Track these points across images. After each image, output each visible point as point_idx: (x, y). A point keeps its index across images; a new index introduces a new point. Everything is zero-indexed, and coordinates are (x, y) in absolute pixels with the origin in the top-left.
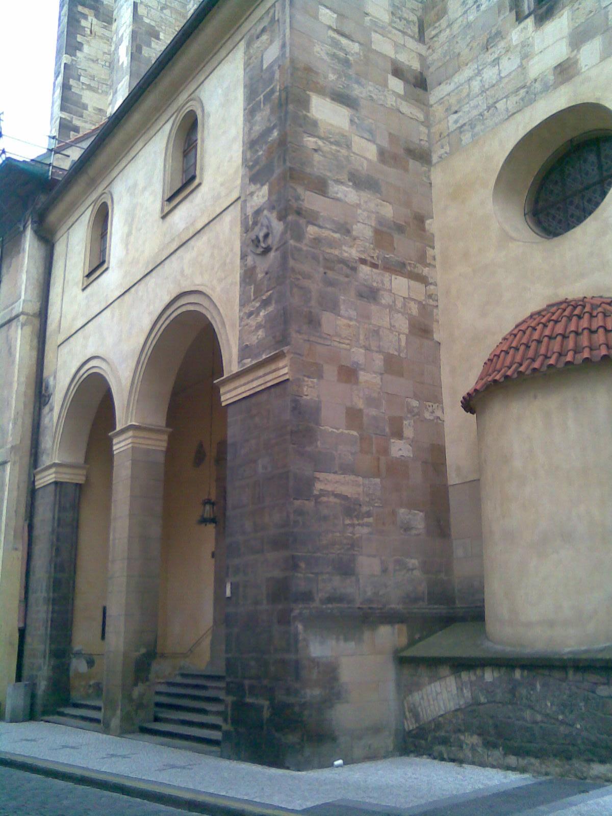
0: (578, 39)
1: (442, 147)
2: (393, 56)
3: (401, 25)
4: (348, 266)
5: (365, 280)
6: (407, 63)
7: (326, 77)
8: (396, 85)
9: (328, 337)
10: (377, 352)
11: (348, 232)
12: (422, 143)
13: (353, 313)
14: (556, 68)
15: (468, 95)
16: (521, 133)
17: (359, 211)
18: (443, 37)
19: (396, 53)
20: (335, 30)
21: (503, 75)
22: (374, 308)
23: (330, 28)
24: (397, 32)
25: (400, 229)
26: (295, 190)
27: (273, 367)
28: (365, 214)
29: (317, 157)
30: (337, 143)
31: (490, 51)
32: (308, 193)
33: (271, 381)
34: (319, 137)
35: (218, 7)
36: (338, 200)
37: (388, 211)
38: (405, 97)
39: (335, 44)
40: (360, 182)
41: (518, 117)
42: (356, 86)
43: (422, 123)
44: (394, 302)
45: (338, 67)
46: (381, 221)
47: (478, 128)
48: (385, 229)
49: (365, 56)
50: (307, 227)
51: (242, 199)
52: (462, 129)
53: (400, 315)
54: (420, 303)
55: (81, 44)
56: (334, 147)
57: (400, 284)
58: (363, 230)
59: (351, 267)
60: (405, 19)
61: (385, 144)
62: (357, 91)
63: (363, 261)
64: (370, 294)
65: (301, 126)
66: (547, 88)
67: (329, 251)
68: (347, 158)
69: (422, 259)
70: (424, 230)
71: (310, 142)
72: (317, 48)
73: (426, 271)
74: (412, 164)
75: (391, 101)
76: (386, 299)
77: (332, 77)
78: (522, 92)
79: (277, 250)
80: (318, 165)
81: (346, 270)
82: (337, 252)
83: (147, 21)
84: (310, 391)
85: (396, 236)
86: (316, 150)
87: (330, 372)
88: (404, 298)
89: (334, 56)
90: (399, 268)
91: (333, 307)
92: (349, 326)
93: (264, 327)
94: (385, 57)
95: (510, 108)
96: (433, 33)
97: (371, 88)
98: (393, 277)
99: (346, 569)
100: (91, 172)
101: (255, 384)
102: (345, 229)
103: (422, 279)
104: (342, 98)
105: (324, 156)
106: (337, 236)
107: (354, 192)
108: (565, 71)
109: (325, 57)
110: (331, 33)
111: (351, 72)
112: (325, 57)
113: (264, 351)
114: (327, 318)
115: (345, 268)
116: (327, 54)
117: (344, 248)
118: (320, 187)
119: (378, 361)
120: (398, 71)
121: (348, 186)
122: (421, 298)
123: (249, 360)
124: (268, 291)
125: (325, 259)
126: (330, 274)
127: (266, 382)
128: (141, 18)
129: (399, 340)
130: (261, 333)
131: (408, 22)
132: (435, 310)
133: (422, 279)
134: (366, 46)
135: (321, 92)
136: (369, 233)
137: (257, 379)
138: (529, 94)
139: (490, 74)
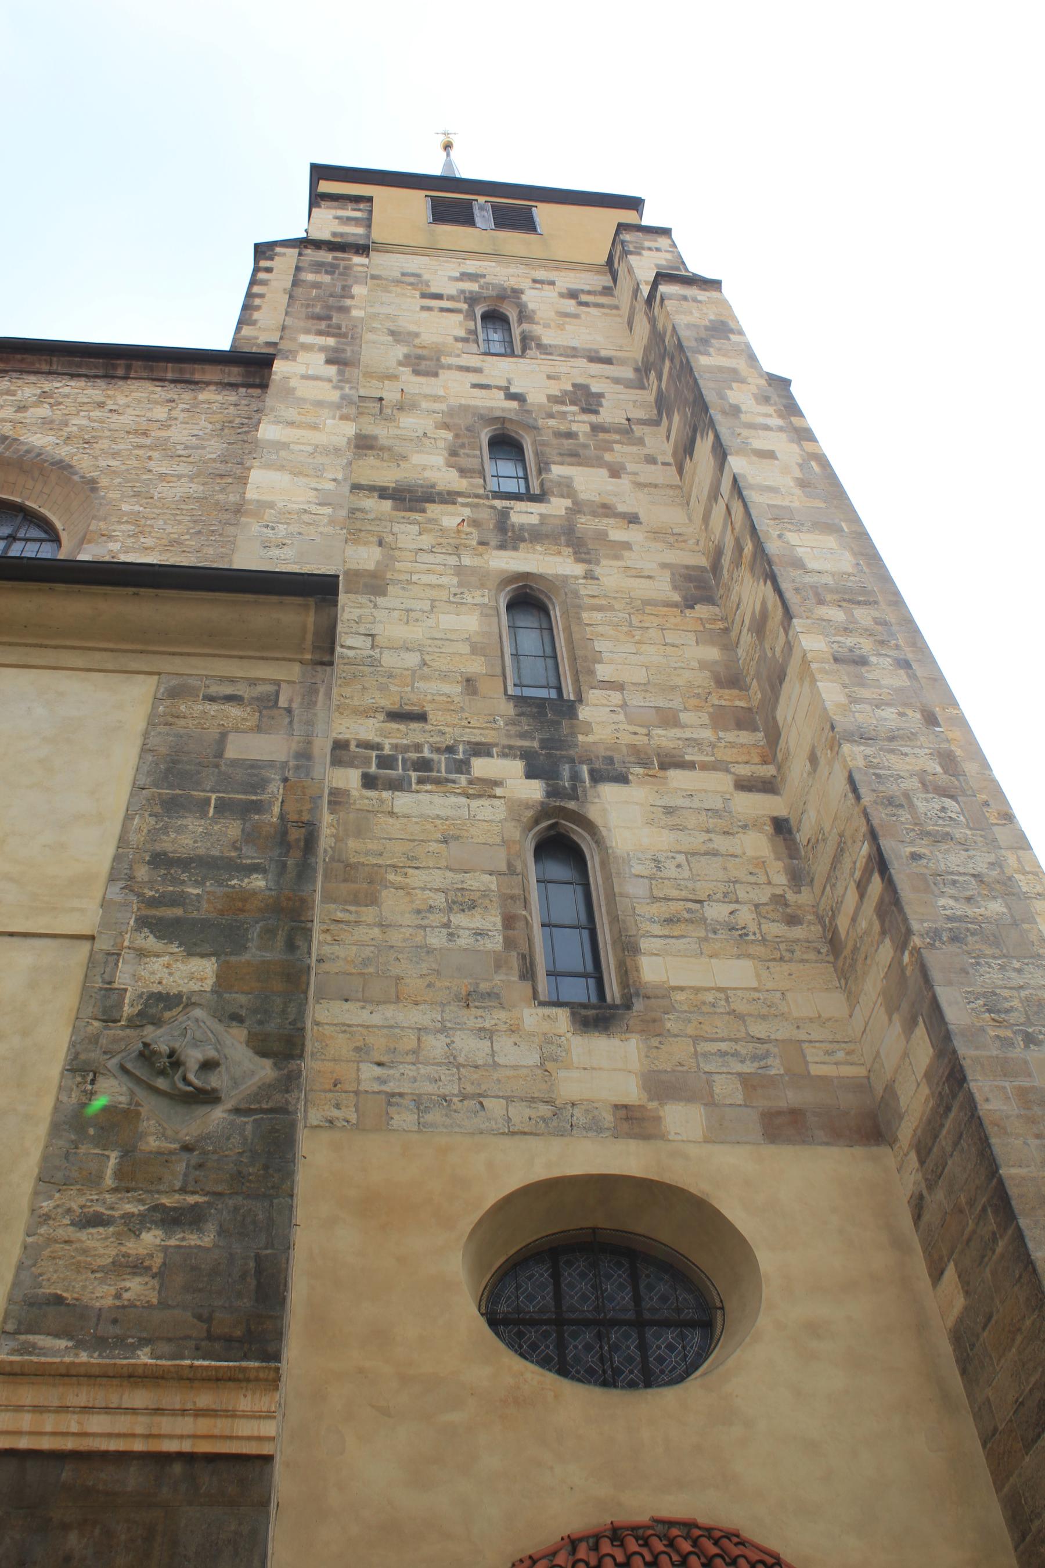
0: (664, 1087)
1: (338, 1106)
14: (616, 1107)
15: (415, 1052)
16: (540, 1173)
18: (363, 933)
21: (500, 1060)
27: (205, 1399)
31: (473, 1011)
33: (171, 1437)
35: (136, 594)
41: (534, 1144)
47: (434, 1116)
51: (103, 944)
52: (394, 1100)
66: (595, 1127)
78: (544, 1110)
79: (237, 1111)
93: (159, 1275)
95: (515, 1120)
96: (340, 915)
101: (97, 1423)
108: (633, 1122)
113: (144, 1342)
123: (62, 1343)
124: (183, 1190)
127: (230, 1438)
130: (136, 1288)
137: (107, 1410)
138: (560, 1120)
139: (469, 1046)
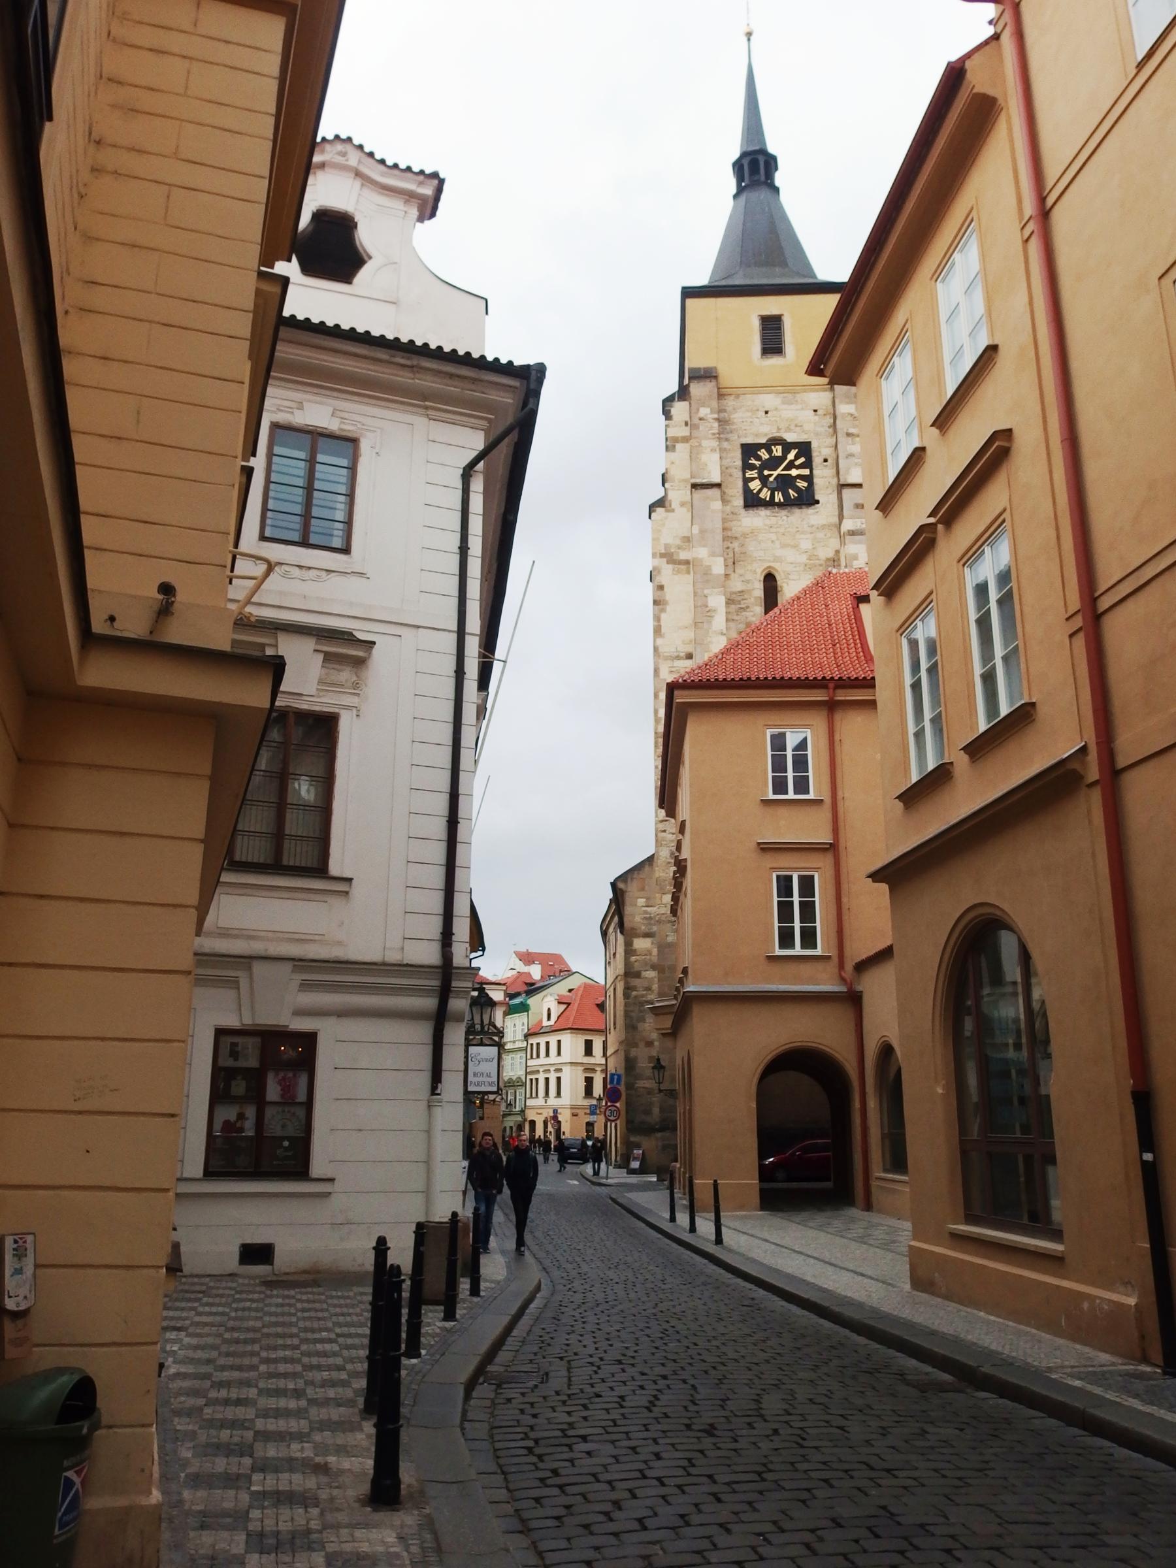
39: (646, 912)
80: (637, 967)
84: (634, 1052)
87: (641, 1045)
89: (646, 918)
91: (644, 1021)
99: (648, 1112)
102: (649, 989)
104: (647, 935)
114: (640, 1026)
118: (638, 975)
135: (638, 936)
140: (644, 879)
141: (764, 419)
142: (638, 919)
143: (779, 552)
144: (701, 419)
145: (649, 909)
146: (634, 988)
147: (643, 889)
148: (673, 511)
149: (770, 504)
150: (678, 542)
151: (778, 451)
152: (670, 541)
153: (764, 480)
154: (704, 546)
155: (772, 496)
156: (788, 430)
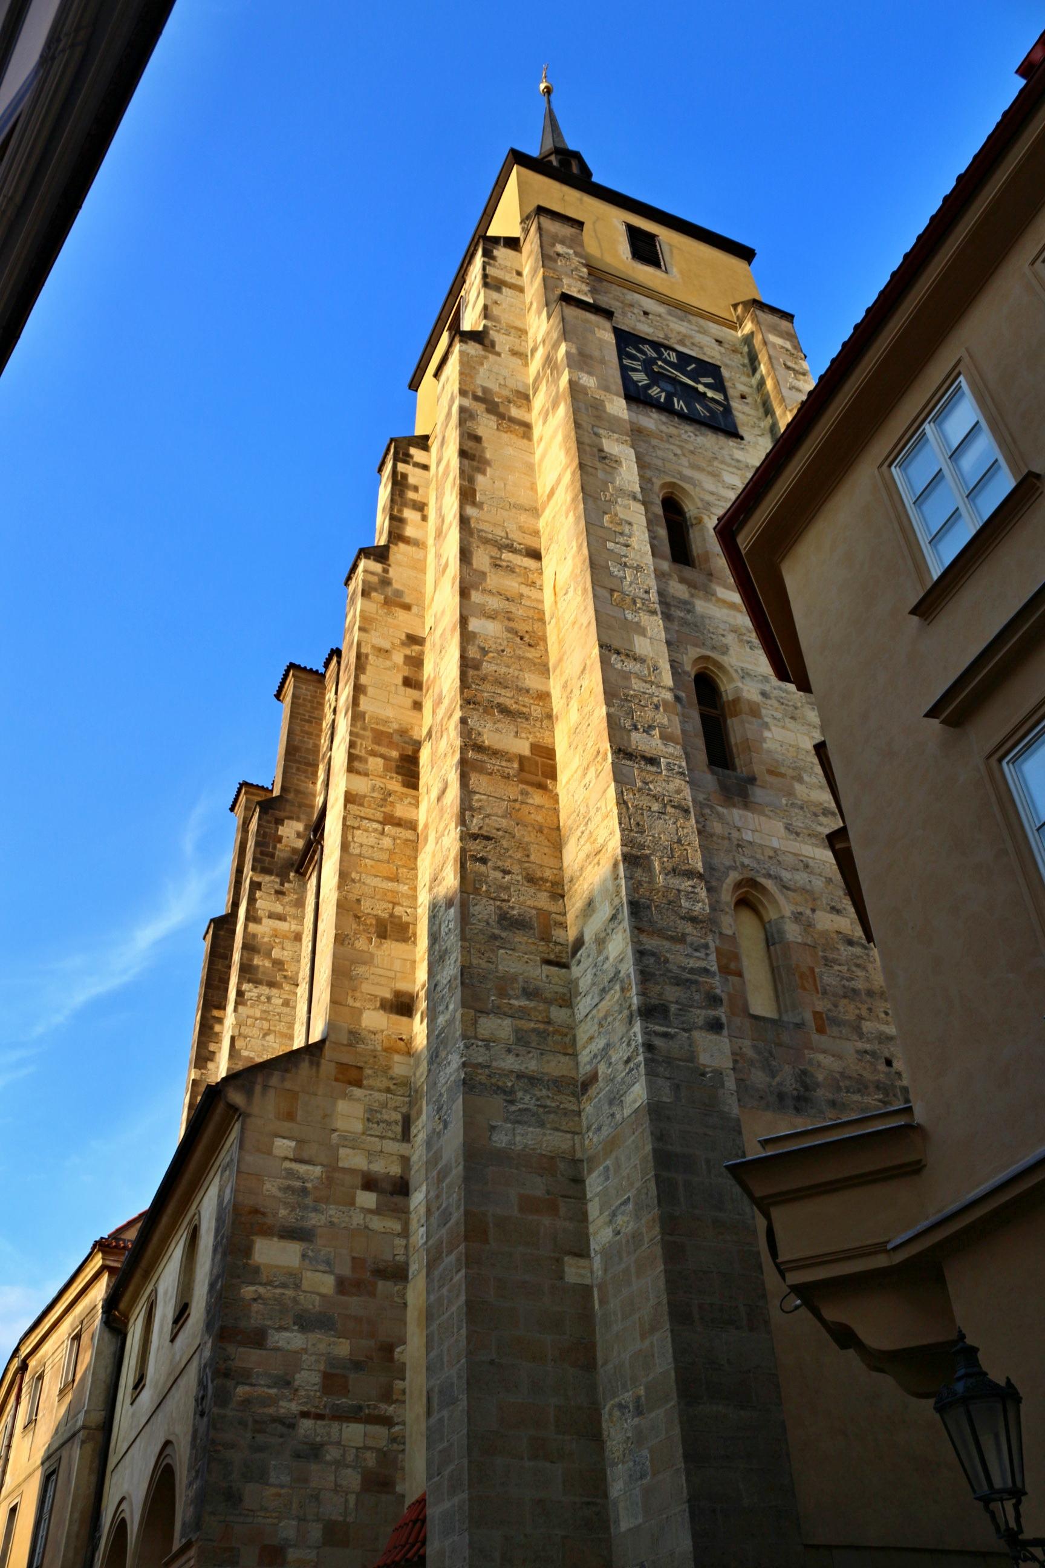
2: (365, 1168)
3: (377, 1130)
4: (283, 1424)
5: (305, 1437)
6: (383, 1171)
7: (275, 1215)
8: (368, 1199)
9: (251, 1513)
10: (314, 1521)
11: (288, 1384)
12: (398, 1258)
13: (285, 1479)
17: (305, 1357)
19: (370, 1162)
20: (291, 1160)
22: (314, 1467)
23: (286, 1158)
24: (373, 1139)
25: (357, 1366)
26: (224, 1349)
28: (313, 1358)
29: (255, 1307)
30: (284, 1286)
32: (241, 1349)
34: (261, 1284)
36: (277, 1349)
37: (343, 1349)
38: (377, 1212)
39: (291, 1174)
40: (305, 1322)
42: (313, 1215)
43: (399, 1235)
44: (343, 1456)
45: (292, 1199)
46: (333, 1361)
48: (338, 1371)
49: (328, 1178)
50: (235, 1388)
53: (349, 1470)
54: (378, 1450)
55: (214, 1053)
56: (278, 1291)
57: (354, 1433)
58: (308, 1379)
59: (289, 1424)
60: (383, 1122)
61: (346, 1271)
62: (314, 1220)
63: (305, 1415)
64: (314, 1451)
65: (239, 1277)
67: (260, 1411)
68: (295, 1300)
69: (387, 1396)
70: (391, 1359)
71: (248, 1291)
72: (268, 1186)
73: (391, 1410)
74: (382, 1286)
75: (358, 1219)
76: (332, 1453)
77: (283, 1212)
81: (280, 1429)
82: (271, 1411)
83: (245, 1053)
85: (352, 1376)
86: (255, 1300)
88: (357, 1449)
89: (288, 1188)
90: (355, 1415)
91: (261, 1476)
92: (280, 1495)
94: (352, 1171)
97: (331, 1212)
98: (345, 1425)
100: (144, 1263)
102: (285, 1382)
103: (387, 1421)
105: (264, 1304)
106: (273, 1391)
107: (299, 1335)
109: (280, 1194)
110: (287, 1164)
111: (308, 1201)
112: (280, 1194)
115: (280, 1427)
116: (280, 1189)
117: (281, 1403)
118: (258, 1339)
119: (316, 1532)
120: (370, 1183)
121: (292, 1331)
122: (383, 1444)
125: (256, 1422)
126: (261, 1438)
128: (239, 1051)
129: (346, 1501)
131: (389, 1123)
132: (400, 1456)
133: (387, 1421)
134: (332, 1168)
135: (267, 1232)
136: (316, 1378)
140: (294, 1095)
141: (643, 319)
142: (271, 1187)
143: (688, 472)
144: (559, 255)
145: (302, 1168)
146: (245, 1376)
147: (290, 1116)
148: (499, 354)
149: (666, 408)
150: (506, 392)
151: (673, 358)
152: (493, 386)
153: (656, 378)
154: (590, 374)
155: (669, 397)
156: (681, 342)
